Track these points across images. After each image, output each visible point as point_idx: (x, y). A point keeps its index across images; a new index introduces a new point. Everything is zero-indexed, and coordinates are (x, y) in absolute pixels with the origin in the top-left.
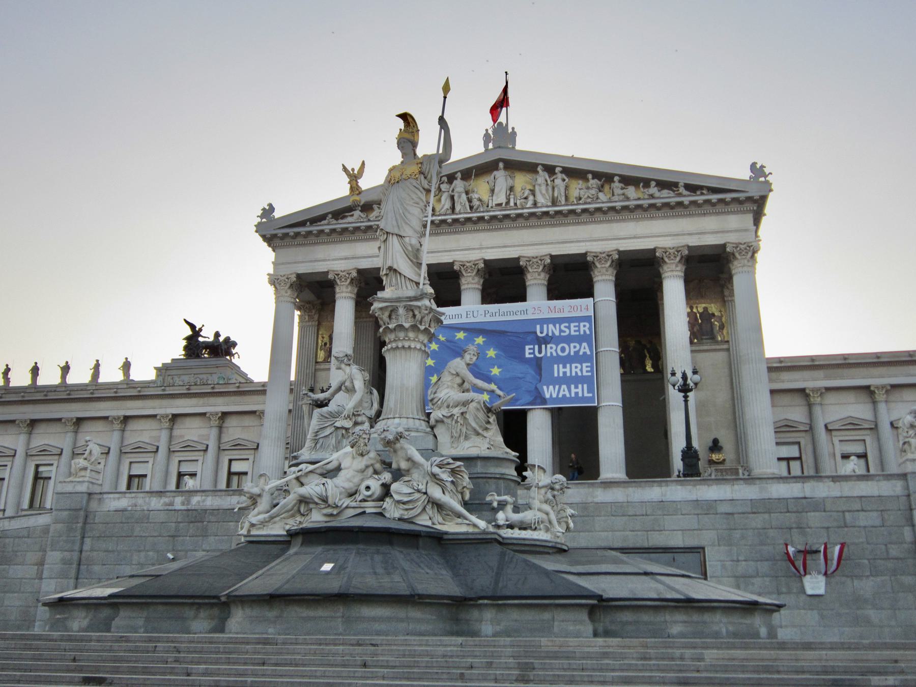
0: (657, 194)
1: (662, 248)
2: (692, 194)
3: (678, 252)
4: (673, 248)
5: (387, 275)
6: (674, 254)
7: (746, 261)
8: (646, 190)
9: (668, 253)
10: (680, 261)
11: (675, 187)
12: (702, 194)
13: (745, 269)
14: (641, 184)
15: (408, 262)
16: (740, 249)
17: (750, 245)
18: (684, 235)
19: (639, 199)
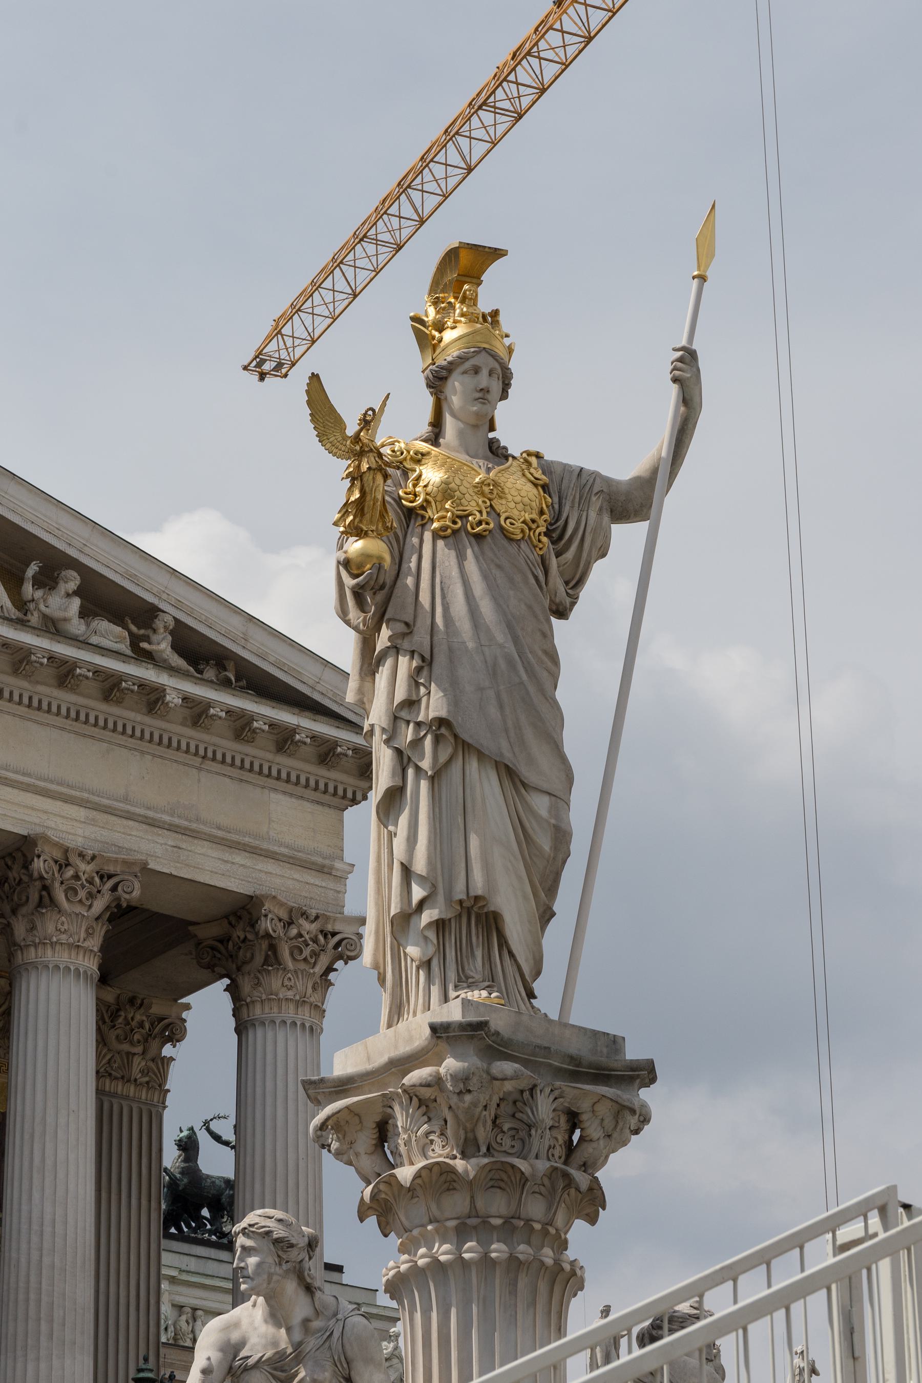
0: (77, 627)
1: (56, 845)
2: (191, 669)
3: (105, 876)
4: (93, 858)
5: (440, 925)
6: (91, 882)
7: (310, 990)
8: (39, 594)
9: (70, 872)
10: (97, 919)
11: (139, 628)
12: (225, 684)
13: (305, 1015)
14: (33, 569)
15: (525, 897)
16: (300, 935)
17: (329, 928)
18: (129, 816)
19: (21, 623)
